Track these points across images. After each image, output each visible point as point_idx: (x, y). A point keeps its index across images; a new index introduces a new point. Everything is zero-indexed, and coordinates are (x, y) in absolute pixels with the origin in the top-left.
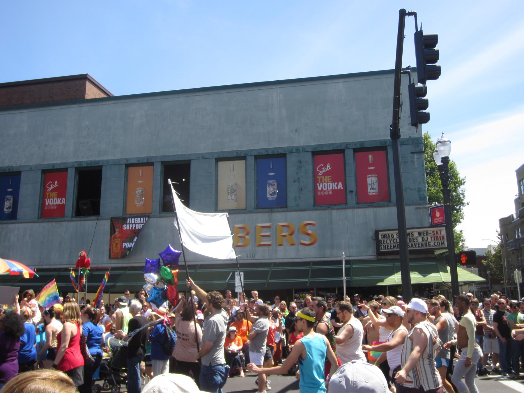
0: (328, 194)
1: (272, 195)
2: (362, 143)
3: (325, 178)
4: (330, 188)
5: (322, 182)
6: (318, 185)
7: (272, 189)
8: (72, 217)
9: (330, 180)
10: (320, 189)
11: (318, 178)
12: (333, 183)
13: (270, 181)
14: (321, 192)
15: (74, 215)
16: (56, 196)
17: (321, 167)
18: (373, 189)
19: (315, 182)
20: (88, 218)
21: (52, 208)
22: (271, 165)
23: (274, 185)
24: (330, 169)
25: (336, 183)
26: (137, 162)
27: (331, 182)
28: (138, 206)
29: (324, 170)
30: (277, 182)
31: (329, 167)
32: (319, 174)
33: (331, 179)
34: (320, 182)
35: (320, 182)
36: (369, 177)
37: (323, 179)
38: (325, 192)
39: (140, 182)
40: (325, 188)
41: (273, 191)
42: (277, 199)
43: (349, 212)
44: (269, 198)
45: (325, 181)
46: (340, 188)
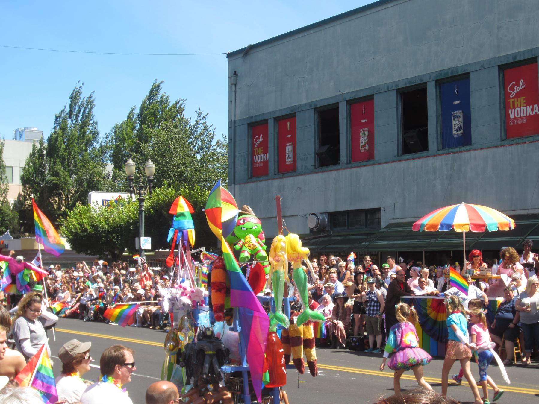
0: (522, 123)
1: (458, 131)
2: (515, 56)
3: (517, 101)
4: (524, 114)
5: (514, 107)
6: (510, 110)
7: (457, 123)
8: (438, 150)
9: (524, 103)
10: (512, 117)
11: (510, 102)
12: (528, 107)
13: (455, 113)
14: (513, 120)
15: (401, 152)
16: (262, 152)
17: (513, 85)
18: (289, 158)
19: (505, 107)
20: (329, 168)
21: (260, 165)
22: (363, 109)
23: (460, 117)
24: (523, 87)
25: (531, 106)
26: (290, 113)
27: (525, 105)
28: (362, 151)
29: (517, 89)
30: (463, 112)
31: (522, 85)
32: (511, 97)
33: (524, 101)
34: (511, 107)
35: (511, 107)
36: (287, 146)
37: (516, 103)
38: (518, 120)
39: (364, 121)
40: (518, 115)
41: (459, 126)
42: (463, 135)
43: (431, 161)
44: (455, 134)
45: (517, 105)
46: (536, 113)
